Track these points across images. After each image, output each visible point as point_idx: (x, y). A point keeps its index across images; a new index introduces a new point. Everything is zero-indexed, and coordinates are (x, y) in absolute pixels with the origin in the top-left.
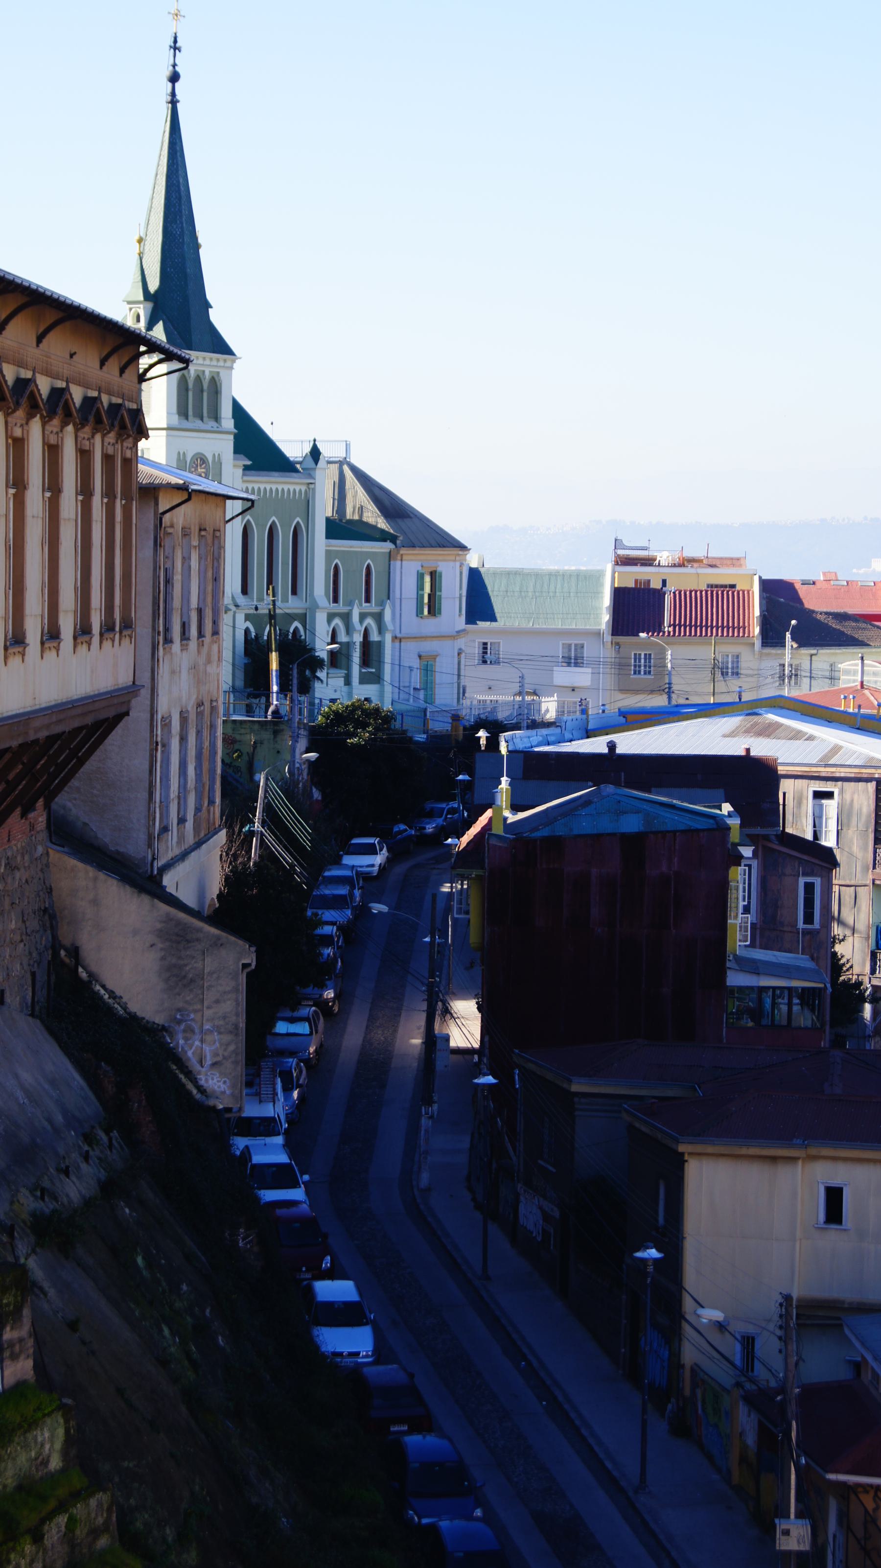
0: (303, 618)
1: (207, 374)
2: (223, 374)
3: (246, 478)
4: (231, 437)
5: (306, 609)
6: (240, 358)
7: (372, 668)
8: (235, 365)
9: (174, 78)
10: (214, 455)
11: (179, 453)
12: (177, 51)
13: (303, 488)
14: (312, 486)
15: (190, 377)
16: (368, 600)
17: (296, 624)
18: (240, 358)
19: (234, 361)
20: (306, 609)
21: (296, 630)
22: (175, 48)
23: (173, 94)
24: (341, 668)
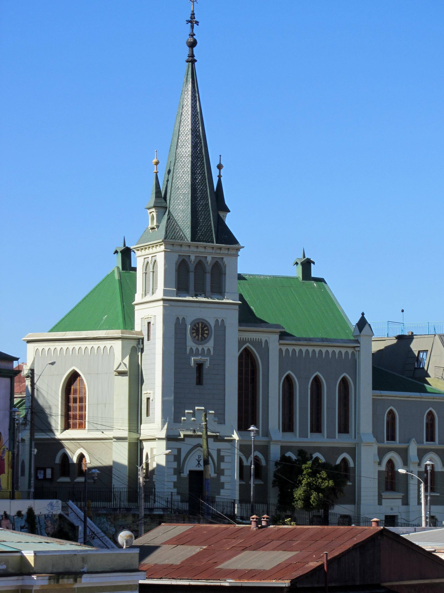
0: (352, 451)
1: (193, 258)
2: (226, 260)
3: (282, 342)
4: (237, 307)
5: (356, 444)
6: (243, 247)
7: (437, 493)
8: (239, 253)
9: (193, 45)
10: (217, 320)
11: (178, 318)
12: (195, 25)
13: (350, 351)
14: (357, 349)
15: (191, 262)
16: (431, 437)
17: (345, 455)
18: (243, 247)
19: (238, 249)
20: (356, 444)
21: (344, 460)
22: (192, 21)
23: (192, 56)
24: (398, 492)
